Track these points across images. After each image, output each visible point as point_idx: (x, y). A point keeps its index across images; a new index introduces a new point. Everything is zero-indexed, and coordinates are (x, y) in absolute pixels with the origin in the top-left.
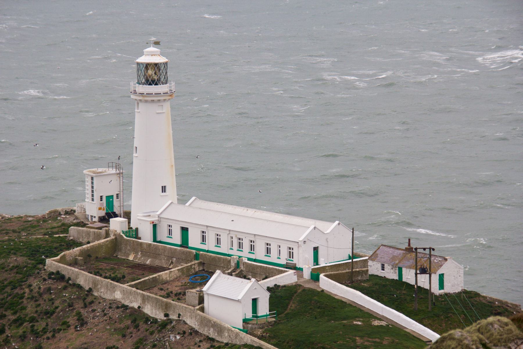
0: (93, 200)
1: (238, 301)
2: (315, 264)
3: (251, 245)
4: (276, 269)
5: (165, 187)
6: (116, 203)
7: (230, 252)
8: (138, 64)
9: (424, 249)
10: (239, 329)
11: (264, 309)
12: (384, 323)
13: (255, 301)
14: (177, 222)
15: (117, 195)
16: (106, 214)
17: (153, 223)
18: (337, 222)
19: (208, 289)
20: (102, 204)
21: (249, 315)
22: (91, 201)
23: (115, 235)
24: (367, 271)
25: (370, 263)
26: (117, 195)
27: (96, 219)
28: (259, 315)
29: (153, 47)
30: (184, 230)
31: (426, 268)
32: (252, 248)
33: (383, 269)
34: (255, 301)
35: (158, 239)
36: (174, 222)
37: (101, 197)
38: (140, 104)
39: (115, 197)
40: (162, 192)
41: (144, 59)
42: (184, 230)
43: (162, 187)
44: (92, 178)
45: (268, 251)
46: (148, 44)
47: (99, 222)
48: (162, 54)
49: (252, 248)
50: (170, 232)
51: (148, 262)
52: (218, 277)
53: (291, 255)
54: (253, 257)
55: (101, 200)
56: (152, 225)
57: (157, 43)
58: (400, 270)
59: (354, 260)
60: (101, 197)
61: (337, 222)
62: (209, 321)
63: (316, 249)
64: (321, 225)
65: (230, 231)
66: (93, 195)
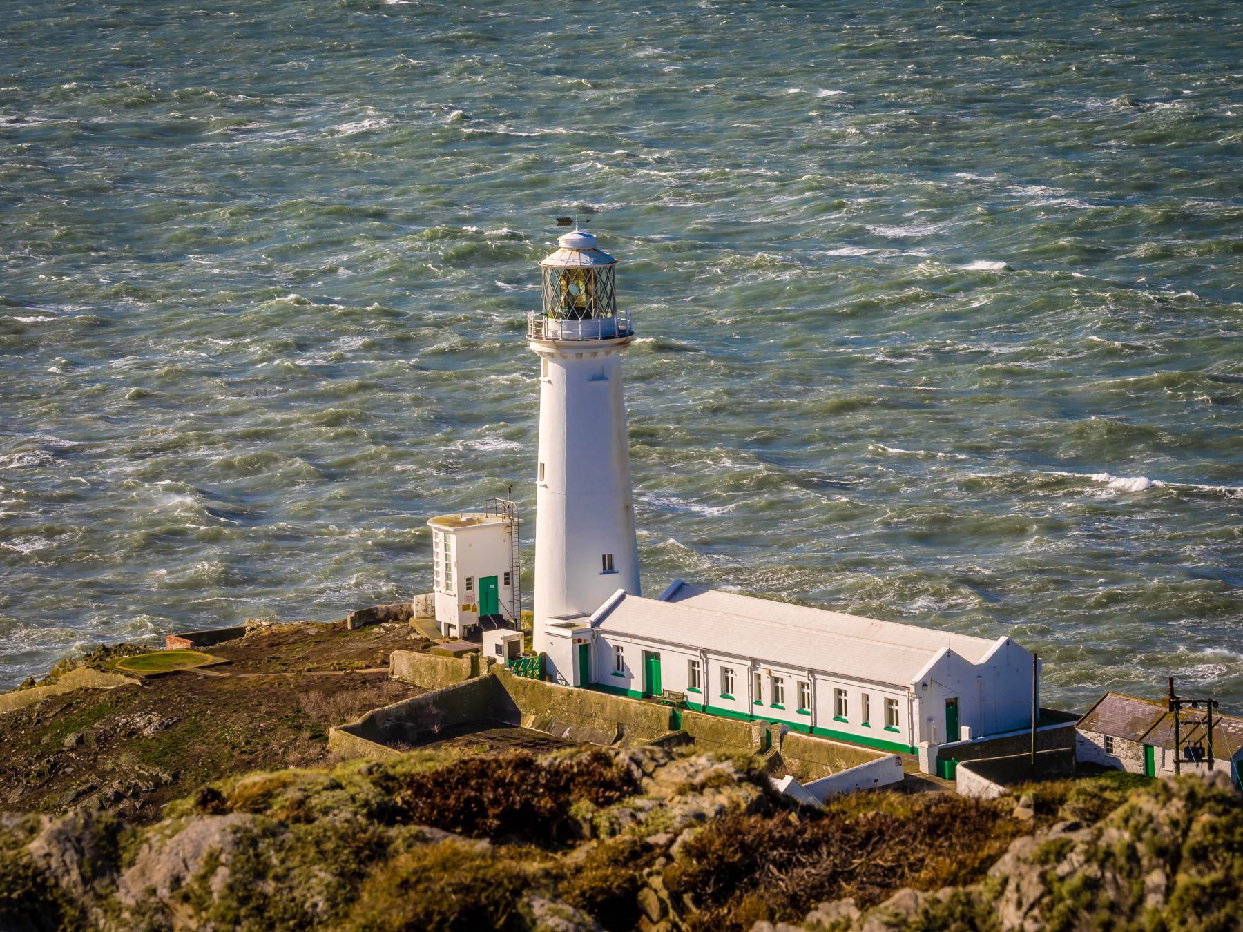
0: (448, 587)
4: (856, 751)
5: (610, 556)
6: (504, 594)
7: (759, 711)
14: (634, 640)
15: (507, 574)
17: (580, 641)
20: (470, 598)
22: (444, 591)
26: (507, 574)
27: (454, 633)
30: (650, 659)
32: (804, 703)
35: (593, 681)
36: (628, 639)
37: (469, 579)
42: (650, 659)
43: (604, 557)
45: (840, 710)
47: (464, 638)
49: (804, 703)
54: (807, 721)
56: (578, 645)
60: (469, 579)
61: (1003, 639)
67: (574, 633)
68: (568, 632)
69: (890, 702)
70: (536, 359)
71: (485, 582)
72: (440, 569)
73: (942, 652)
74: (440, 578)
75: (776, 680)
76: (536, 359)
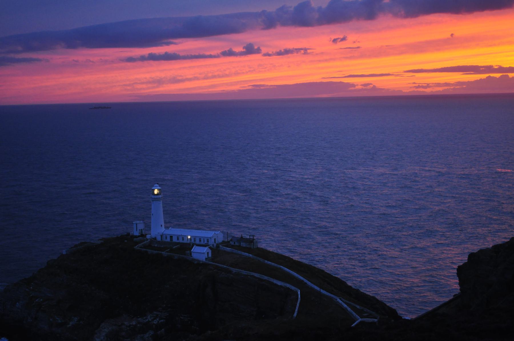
0: (137, 231)
1: (204, 253)
6: (143, 231)
9: (252, 236)
11: (210, 255)
13: (208, 253)
16: (141, 235)
19: (193, 251)
21: (207, 257)
22: (136, 231)
23: (150, 240)
25: (231, 242)
26: (144, 229)
33: (235, 243)
34: (208, 253)
38: (154, 201)
42: (171, 237)
44: (137, 224)
46: (155, 184)
48: (159, 186)
50: (166, 238)
51: (162, 247)
52: (195, 247)
53: (208, 241)
57: (157, 184)
58: (240, 243)
60: (139, 230)
62: (195, 259)
63: (215, 239)
64: (216, 233)
66: (137, 229)
71: (141, 230)
73: (214, 233)
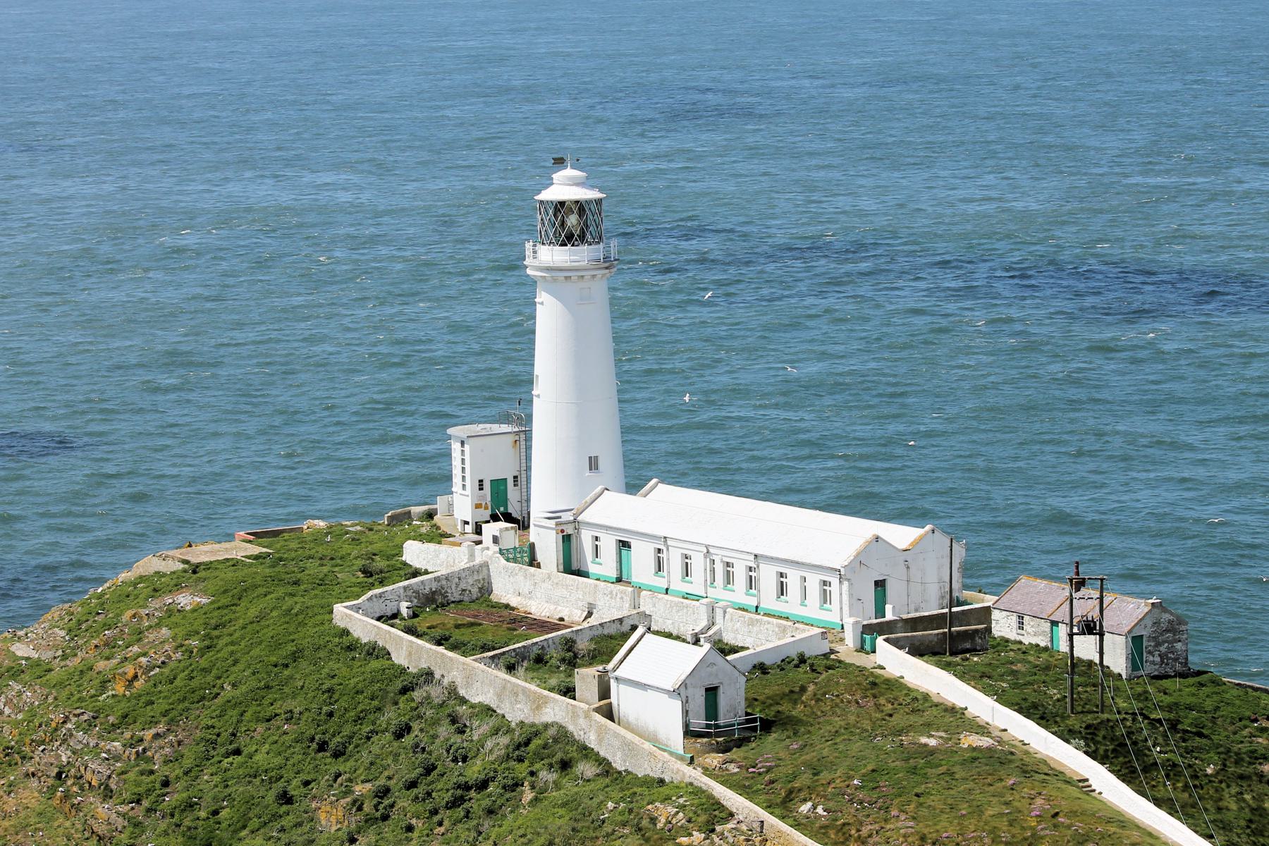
2: (879, 615)
3: (751, 577)
6: (513, 494)
8: (541, 202)
10: (671, 753)
12: (985, 742)
13: (712, 692)
15: (515, 477)
17: (562, 531)
18: (928, 527)
20: (484, 497)
21: (699, 722)
22: (461, 491)
24: (989, 630)
25: (996, 615)
26: (515, 477)
28: (721, 722)
29: (572, 167)
30: (624, 545)
31: (1093, 621)
33: (1021, 625)
34: (712, 692)
35: (575, 567)
37: (481, 481)
39: (510, 482)
40: (591, 469)
41: (552, 194)
42: (624, 545)
43: (590, 458)
44: (463, 443)
45: (782, 590)
52: (642, 636)
55: (481, 489)
56: (561, 535)
59: (954, 609)
60: (481, 481)
61: (928, 527)
65: (707, 547)
67: (557, 524)
68: (552, 523)
69: (825, 583)
70: (533, 283)
71: (494, 483)
72: (456, 472)
73: (869, 536)
74: (457, 480)
75: (728, 564)
76: (531, 285)
